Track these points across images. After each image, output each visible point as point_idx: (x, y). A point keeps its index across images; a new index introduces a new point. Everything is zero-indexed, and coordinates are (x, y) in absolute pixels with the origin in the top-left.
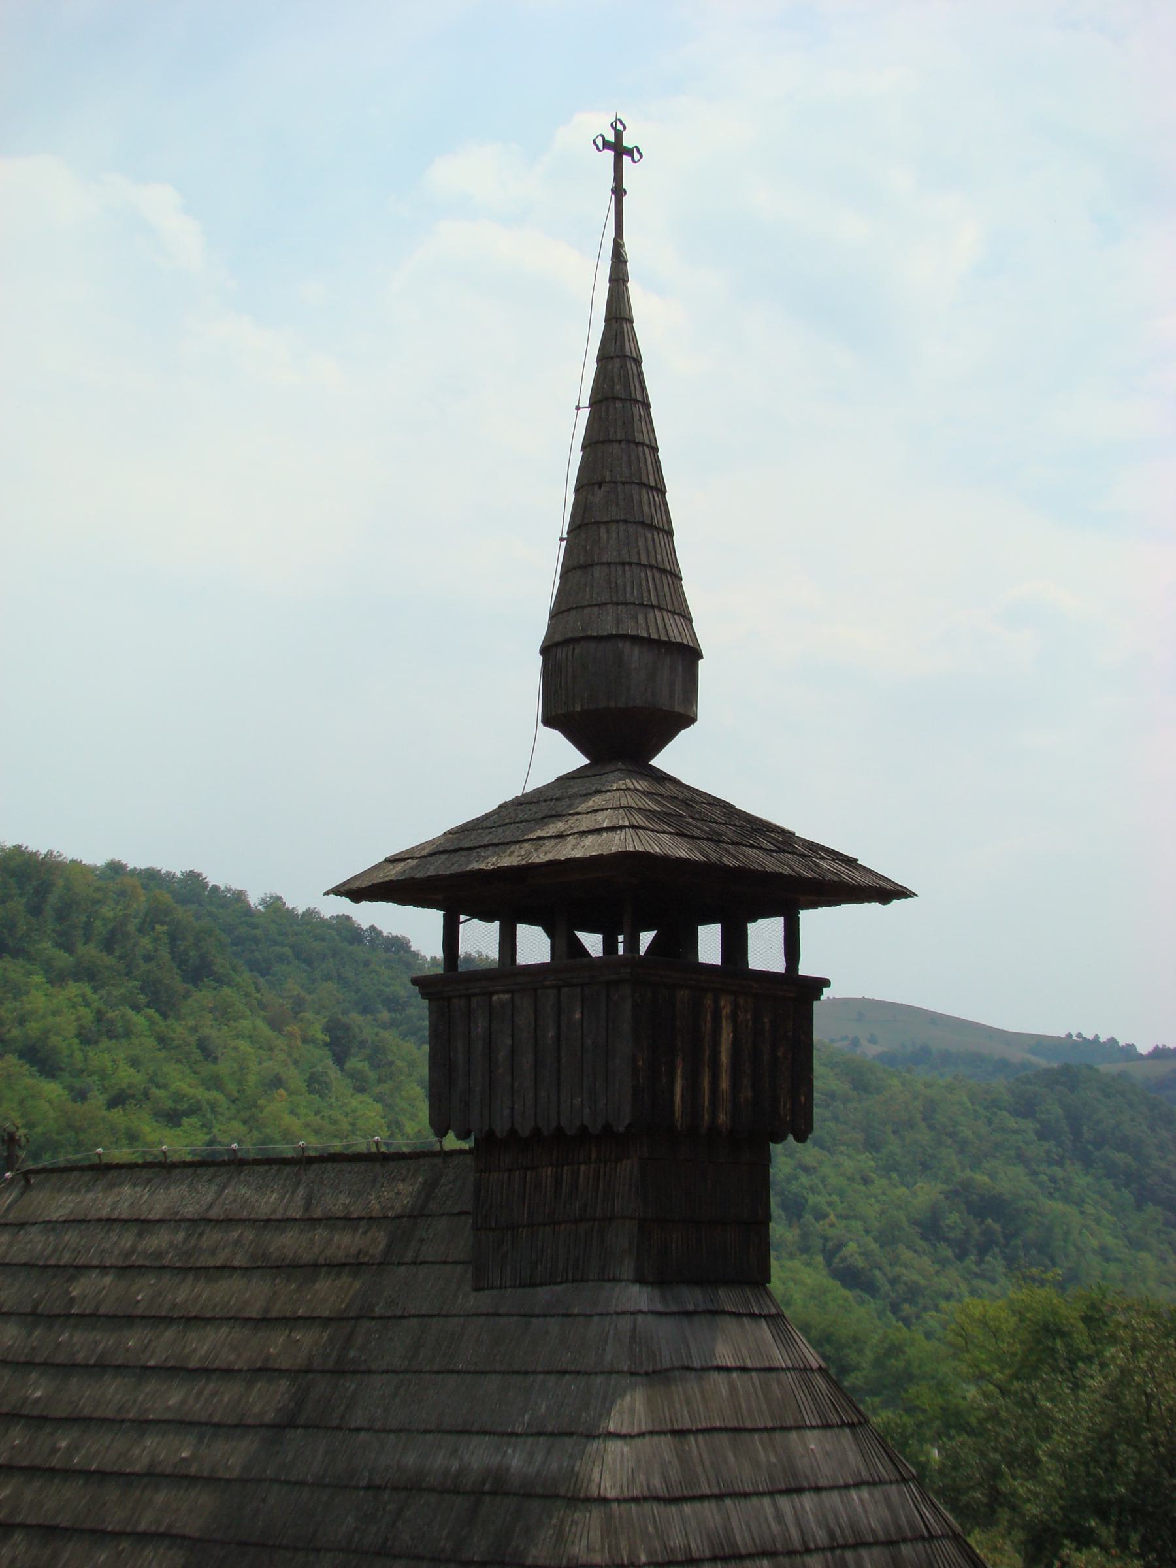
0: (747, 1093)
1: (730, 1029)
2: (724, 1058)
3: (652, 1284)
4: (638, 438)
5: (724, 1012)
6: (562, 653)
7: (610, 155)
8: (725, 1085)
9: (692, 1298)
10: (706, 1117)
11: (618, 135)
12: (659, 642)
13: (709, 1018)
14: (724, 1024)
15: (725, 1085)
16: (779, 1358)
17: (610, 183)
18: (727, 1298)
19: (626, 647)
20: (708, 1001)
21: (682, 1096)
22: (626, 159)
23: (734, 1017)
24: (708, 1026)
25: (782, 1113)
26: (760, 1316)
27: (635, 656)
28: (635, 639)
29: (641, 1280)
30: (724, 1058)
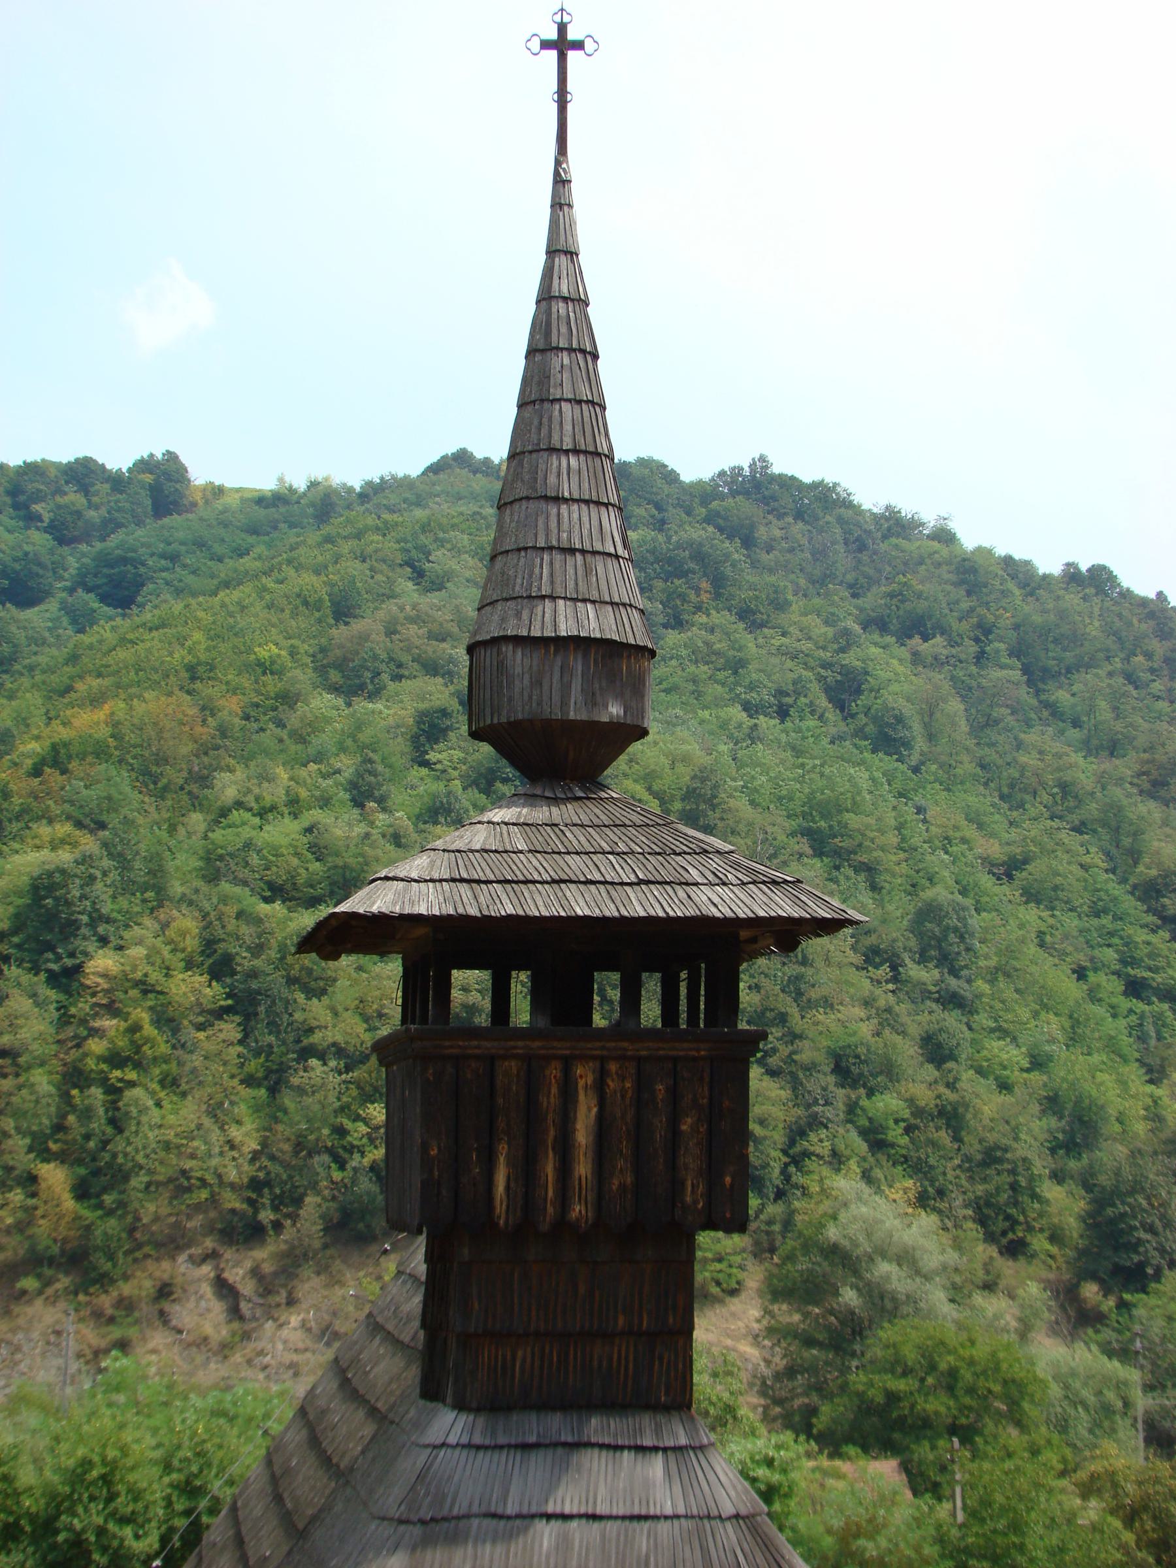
0: (622, 1176)
1: (594, 1102)
2: (583, 1134)
3: (478, 1410)
4: (556, 393)
5: (581, 1083)
6: (487, 657)
7: (553, 54)
8: (583, 1168)
9: (531, 1426)
10: (550, 1210)
11: (562, 28)
12: (544, 641)
13: (554, 1090)
14: (582, 1096)
15: (583, 1168)
16: (666, 1500)
17: (554, 87)
18: (596, 1426)
19: (507, 649)
20: (554, 1071)
21: (508, 1188)
22: (572, 55)
23: (600, 1087)
24: (551, 1097)
25: (688, 1199)
26: (655, 1449)
27: (518, 661)
28: (517, 640)
29: (460, 1406)
30: (583, 1134)
